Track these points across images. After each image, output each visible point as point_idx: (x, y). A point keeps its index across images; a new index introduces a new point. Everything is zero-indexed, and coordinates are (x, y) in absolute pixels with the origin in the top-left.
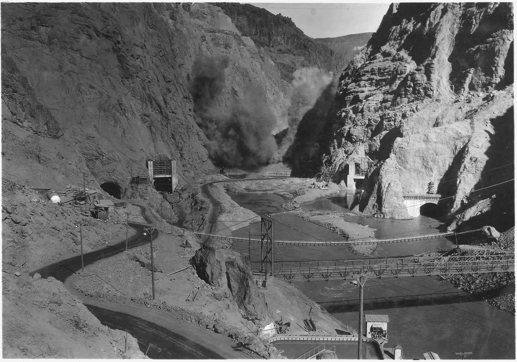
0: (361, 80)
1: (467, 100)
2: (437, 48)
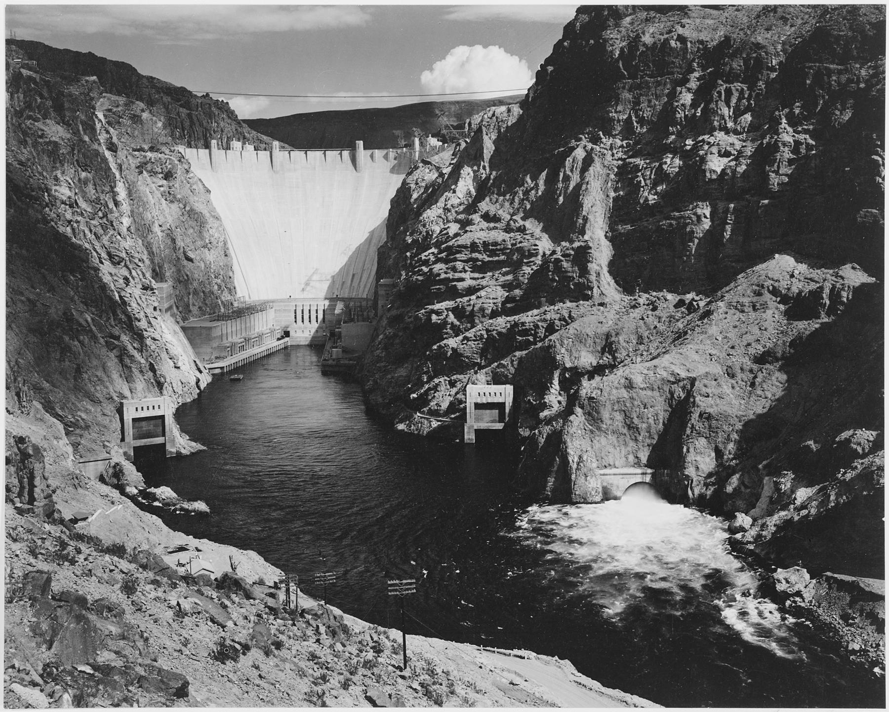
0: (455, 260)
1: (648, 305)
2: (586, 220)
